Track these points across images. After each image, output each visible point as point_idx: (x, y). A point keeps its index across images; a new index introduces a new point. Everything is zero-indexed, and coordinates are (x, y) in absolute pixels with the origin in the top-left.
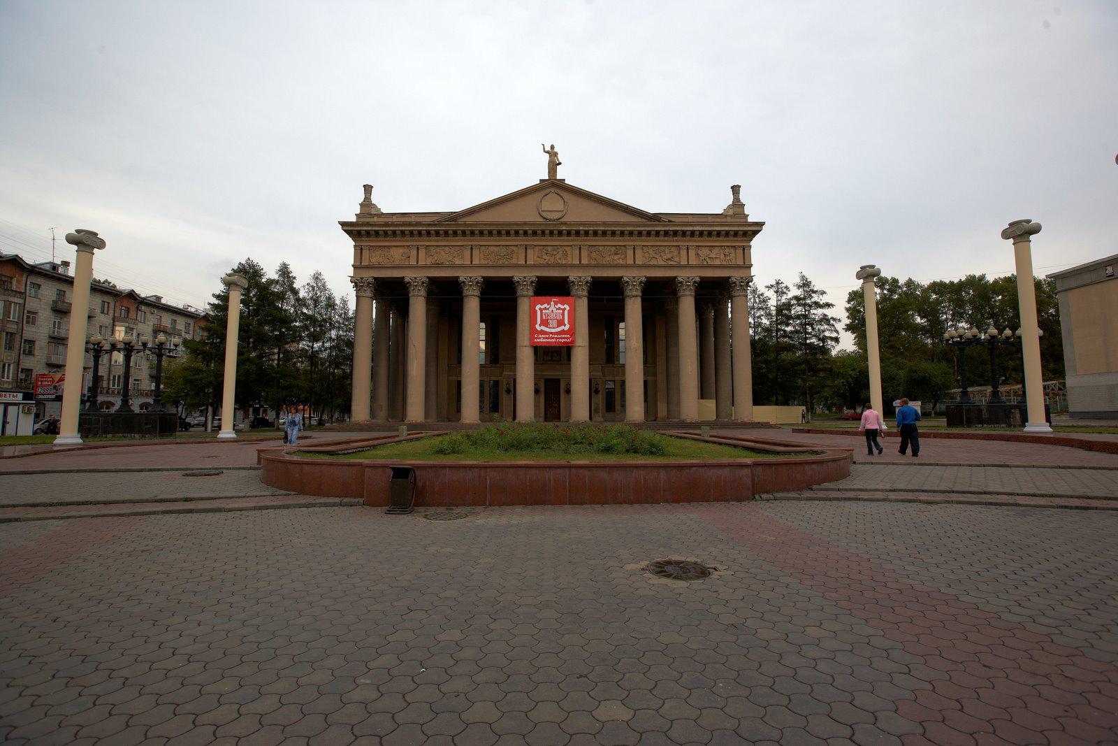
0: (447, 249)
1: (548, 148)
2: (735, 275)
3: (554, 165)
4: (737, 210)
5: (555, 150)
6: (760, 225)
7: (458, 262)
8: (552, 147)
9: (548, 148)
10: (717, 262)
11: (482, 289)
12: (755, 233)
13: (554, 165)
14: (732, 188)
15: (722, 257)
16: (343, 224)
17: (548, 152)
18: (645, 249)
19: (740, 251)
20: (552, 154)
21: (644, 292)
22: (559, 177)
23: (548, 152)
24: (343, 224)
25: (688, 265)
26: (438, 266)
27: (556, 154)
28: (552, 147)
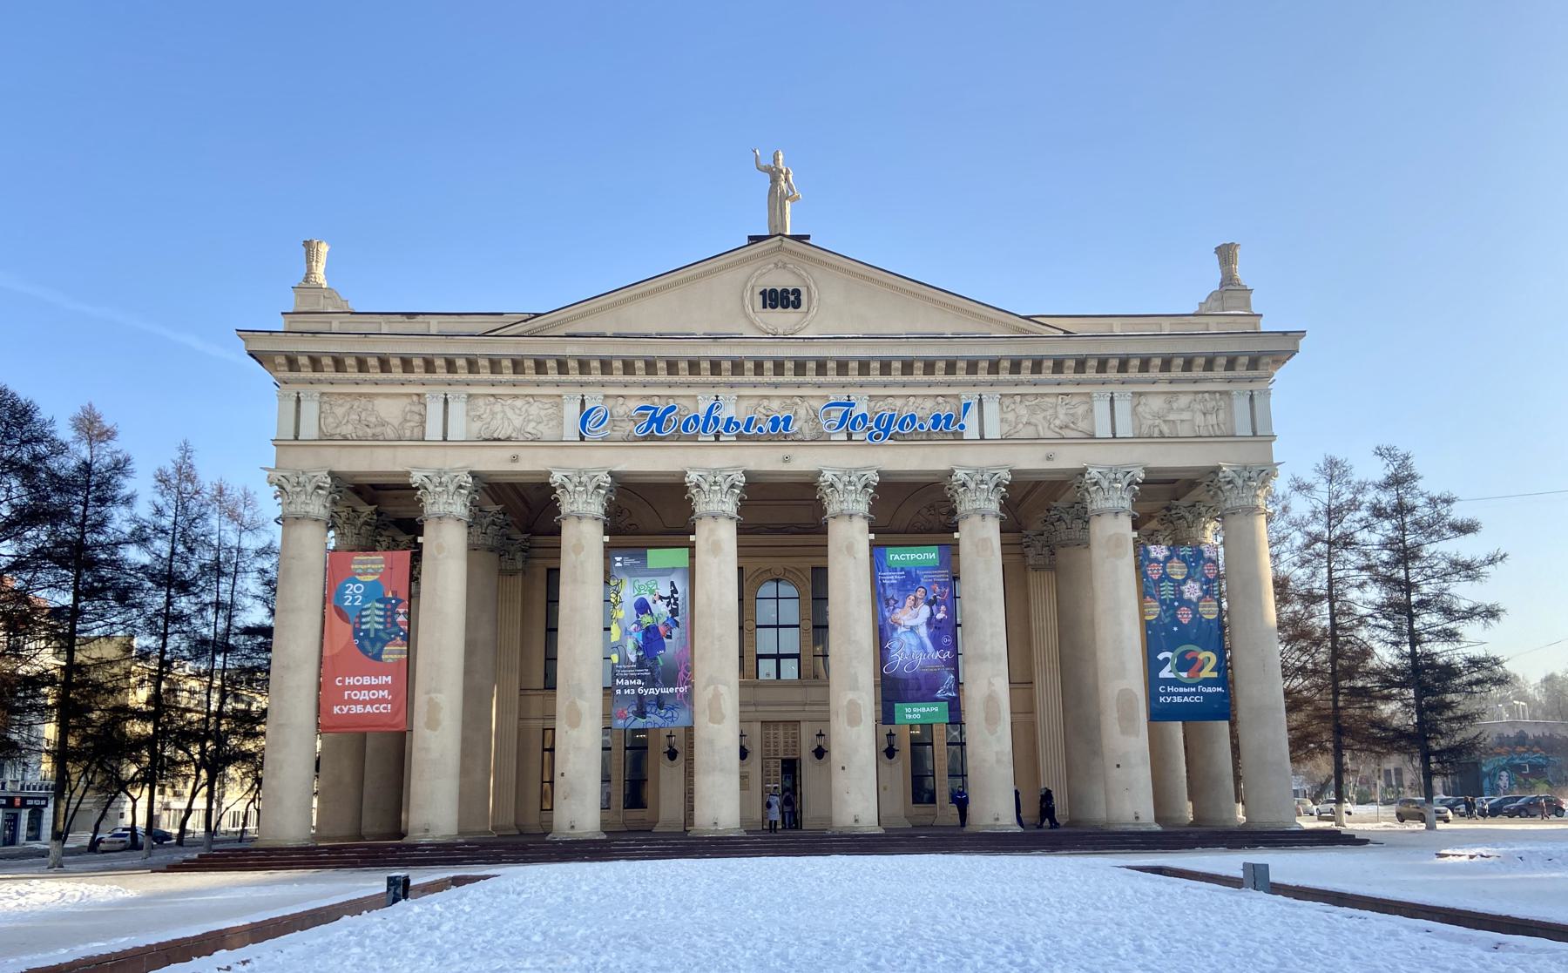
0: (519, 403)
2: (1226, 458)
7: (546, 431)
9: (767, 161)
10: (1184, 430)
11: (609, 501)
13: (776, 200)
14: (1218, 250)
15: (1199, 419)
17: (768, 170)
18: (1007, 401)
19: (1241, 406)
20: (775, 175)
21: (1008, 505)
23: (768, 170)
25: (1108, 440)
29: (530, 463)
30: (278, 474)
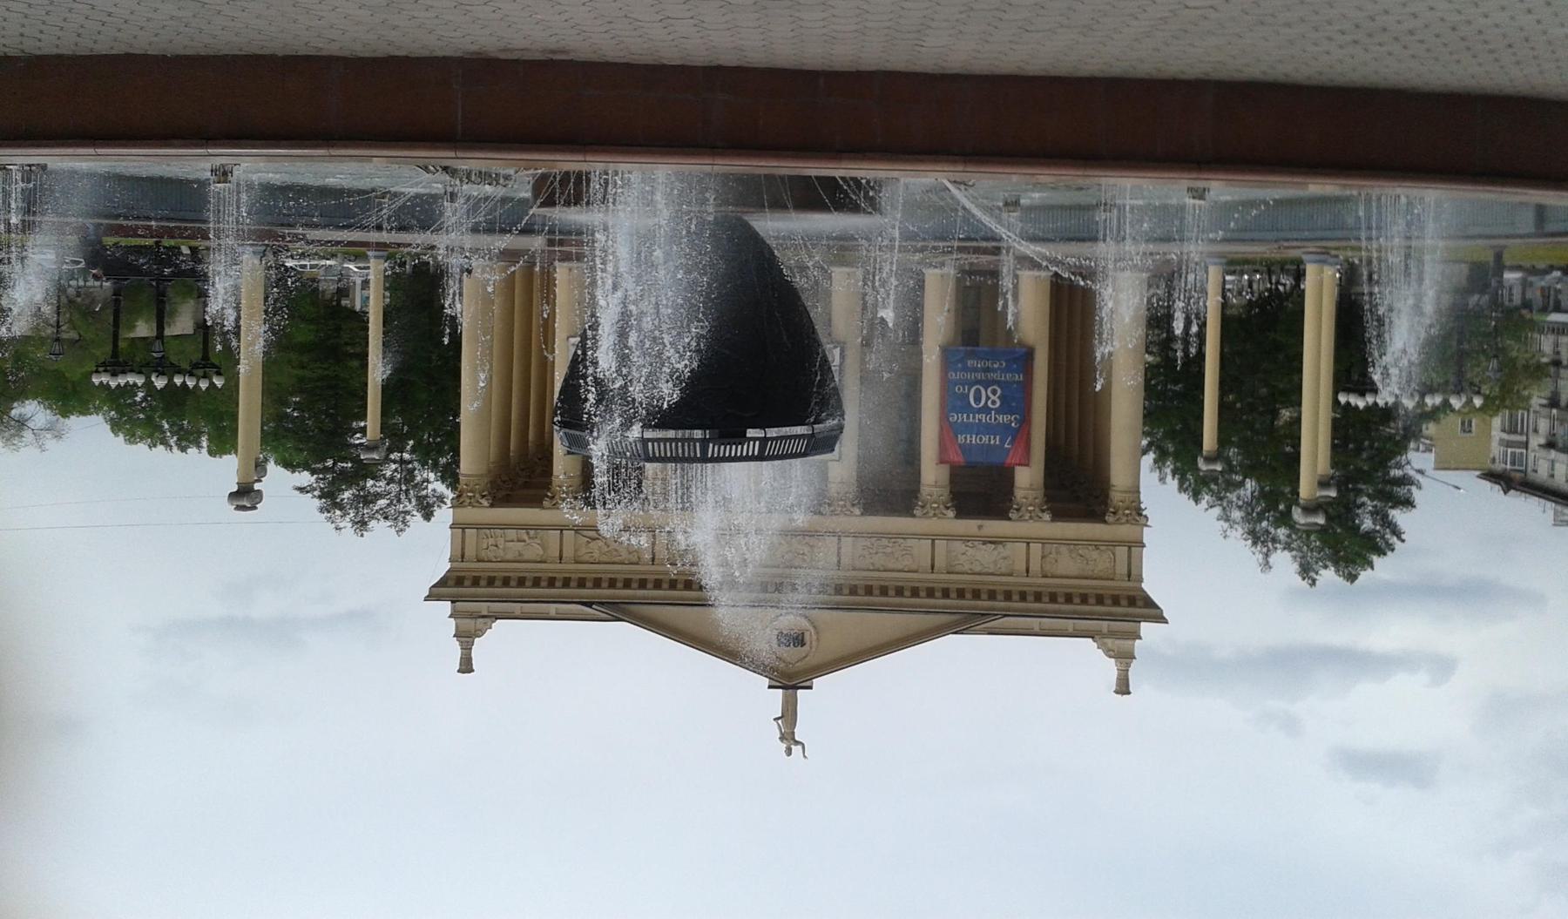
1: (796, 749)
3: (789, 716)
4: (469, 624)
5: (784, 746)
6: (433, 596)
7: (958, 546)
8: (789, 752)
10: (512, 534)
12: (443, 583)
13: (789, 716)
15: (501, 541)
16: (1160, 619)
17: (797, 743)
20: (788, 737)
22: (780, 691)
23: (797, 743)
24: (1160, 619)
26: (995, 541)
27: (782, 738)
28: (789, 752)
29: (970, 526)
30: (1143, 520)
